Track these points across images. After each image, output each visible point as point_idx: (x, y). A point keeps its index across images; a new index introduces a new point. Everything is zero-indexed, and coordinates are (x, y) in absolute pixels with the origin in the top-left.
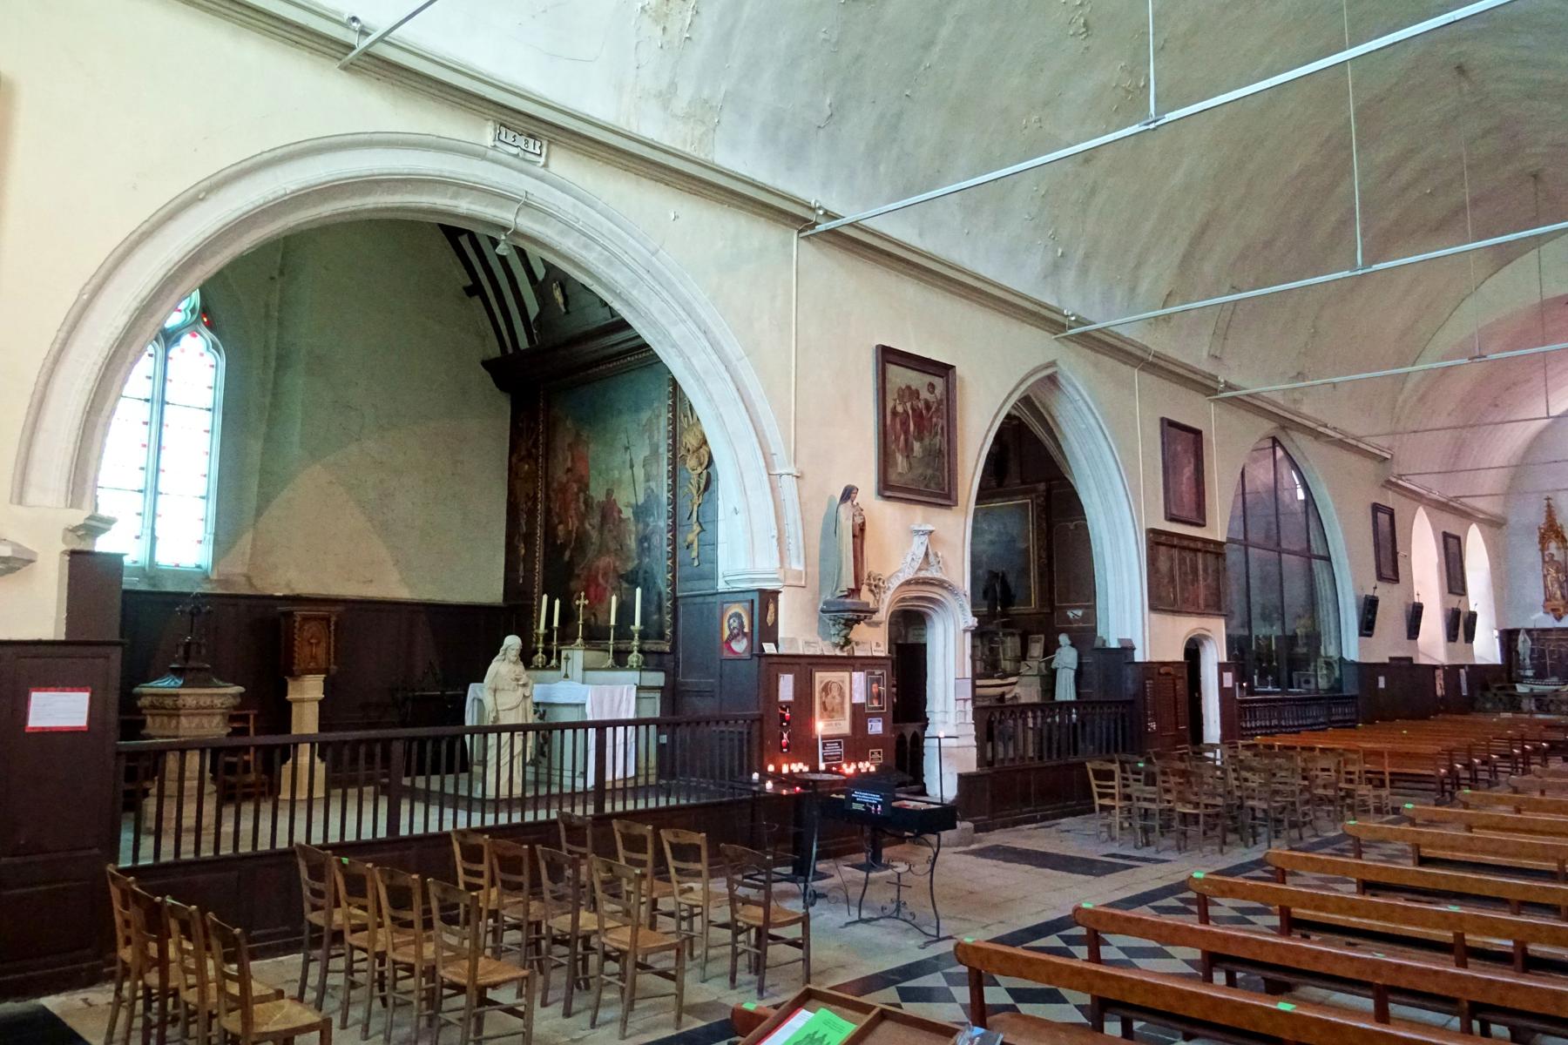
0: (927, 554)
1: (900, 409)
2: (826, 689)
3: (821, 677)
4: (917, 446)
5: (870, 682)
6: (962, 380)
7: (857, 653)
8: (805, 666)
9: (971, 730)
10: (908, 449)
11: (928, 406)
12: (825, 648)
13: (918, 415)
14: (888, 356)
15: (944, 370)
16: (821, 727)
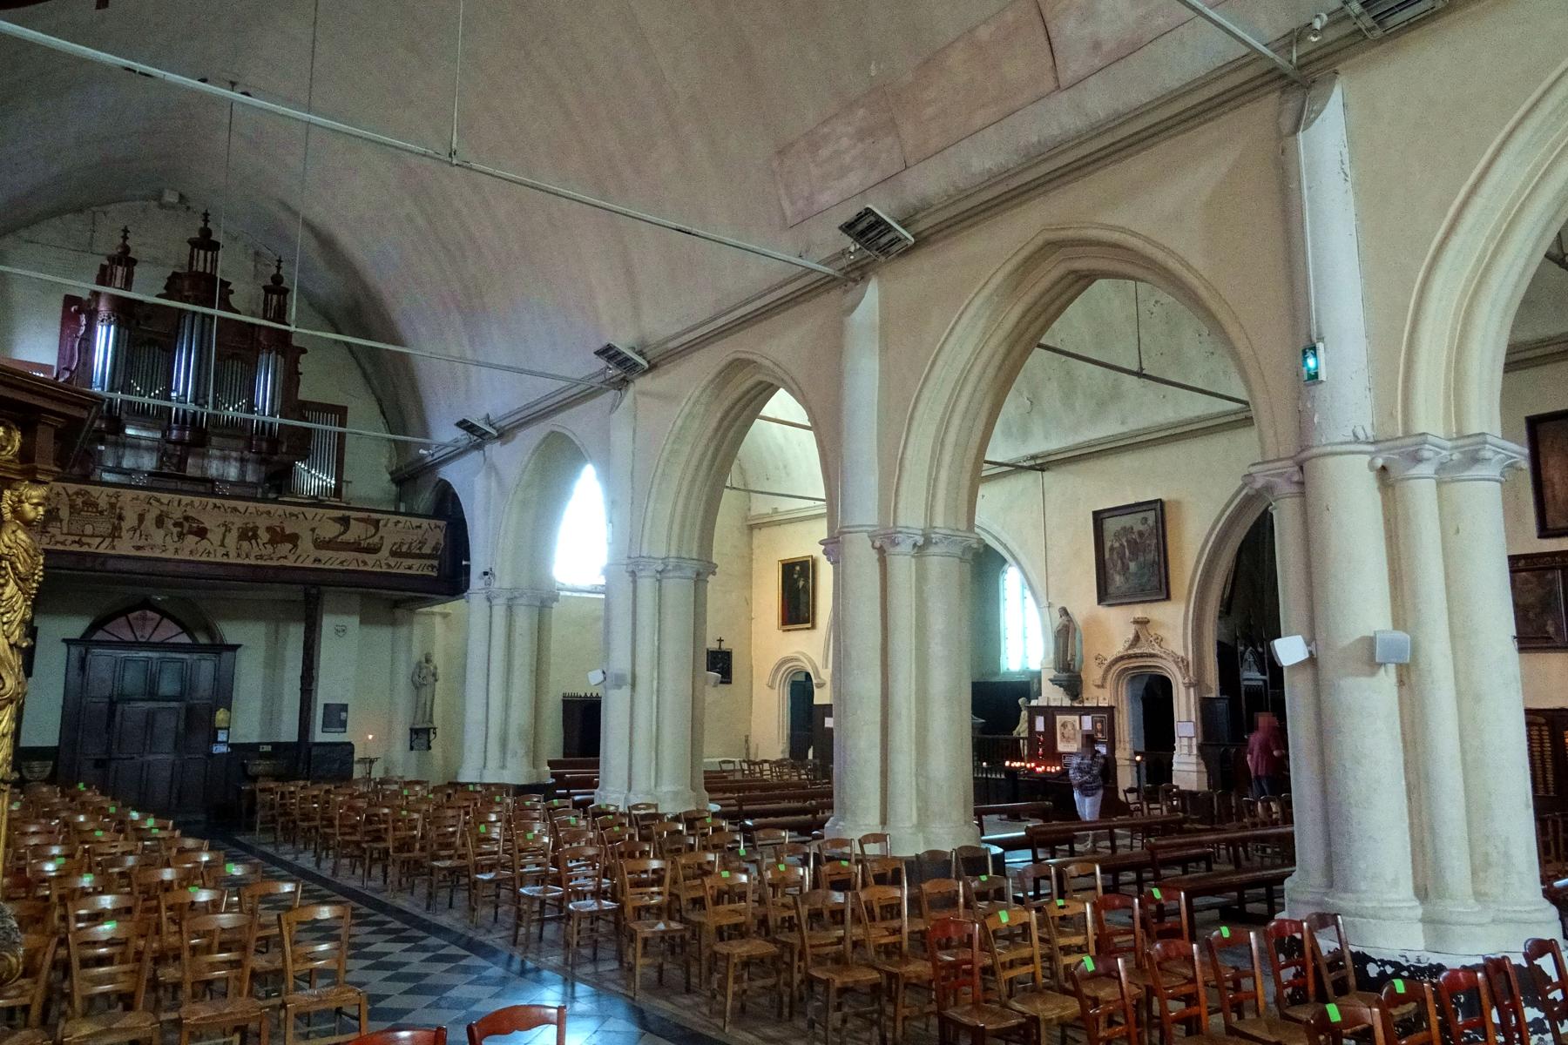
0: (1137, 638)
1: (1117, 545)
2: (1064, 725)
3: (1060, 719)
4: (1132, 566)
5: (1094, 723)
6: (1178, 503)
7: (1087, 704)
8: (1050, 713)
9: (1194, 759)
10: (1125, 568)
11: (1141, 534)
12: (1067, 702)
13: (1133, 545)
14: (1099, 517)
15: (1158, 506)
16: (1062, 747)
